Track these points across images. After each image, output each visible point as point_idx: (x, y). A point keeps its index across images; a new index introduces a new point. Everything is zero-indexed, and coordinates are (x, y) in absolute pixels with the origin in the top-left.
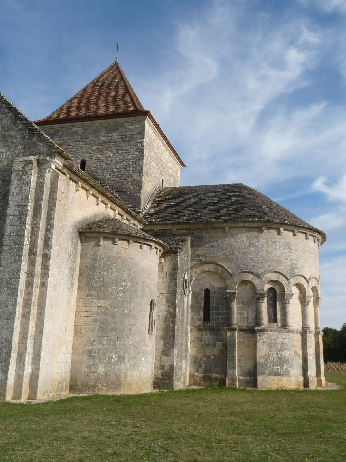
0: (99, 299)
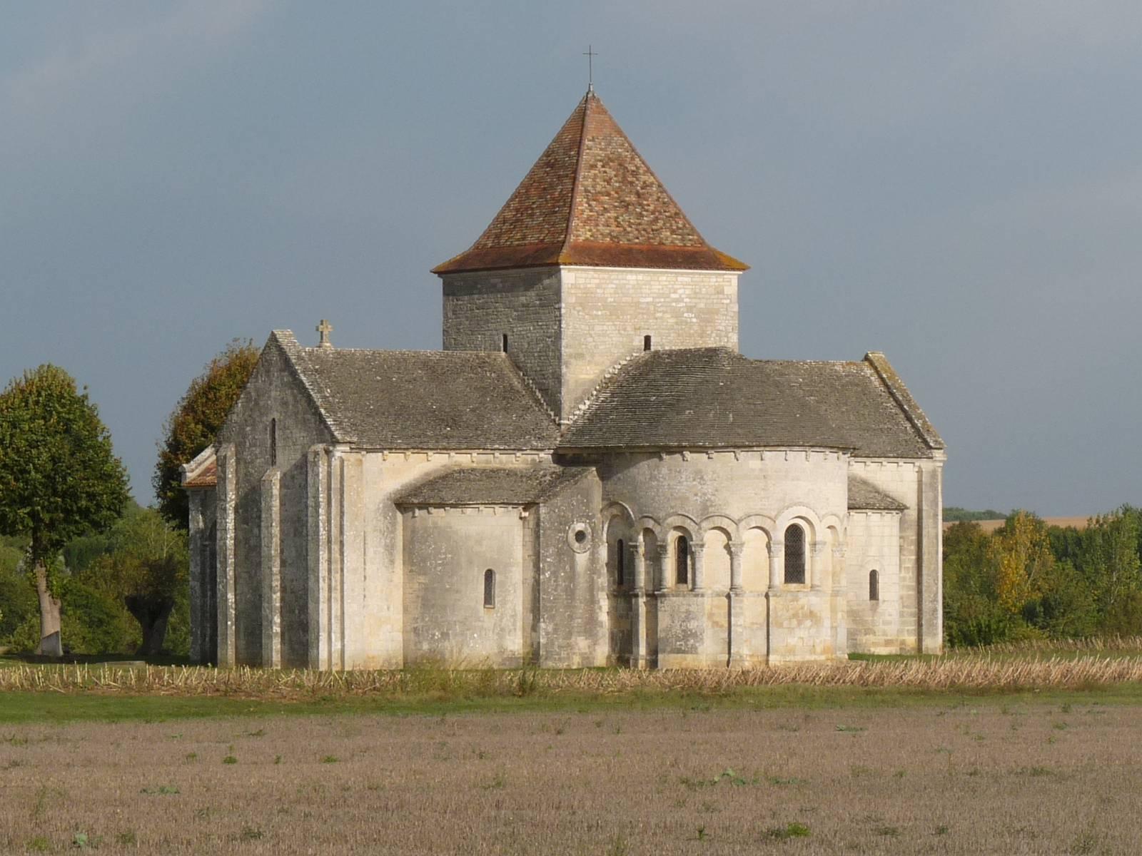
0: (419, 574)
